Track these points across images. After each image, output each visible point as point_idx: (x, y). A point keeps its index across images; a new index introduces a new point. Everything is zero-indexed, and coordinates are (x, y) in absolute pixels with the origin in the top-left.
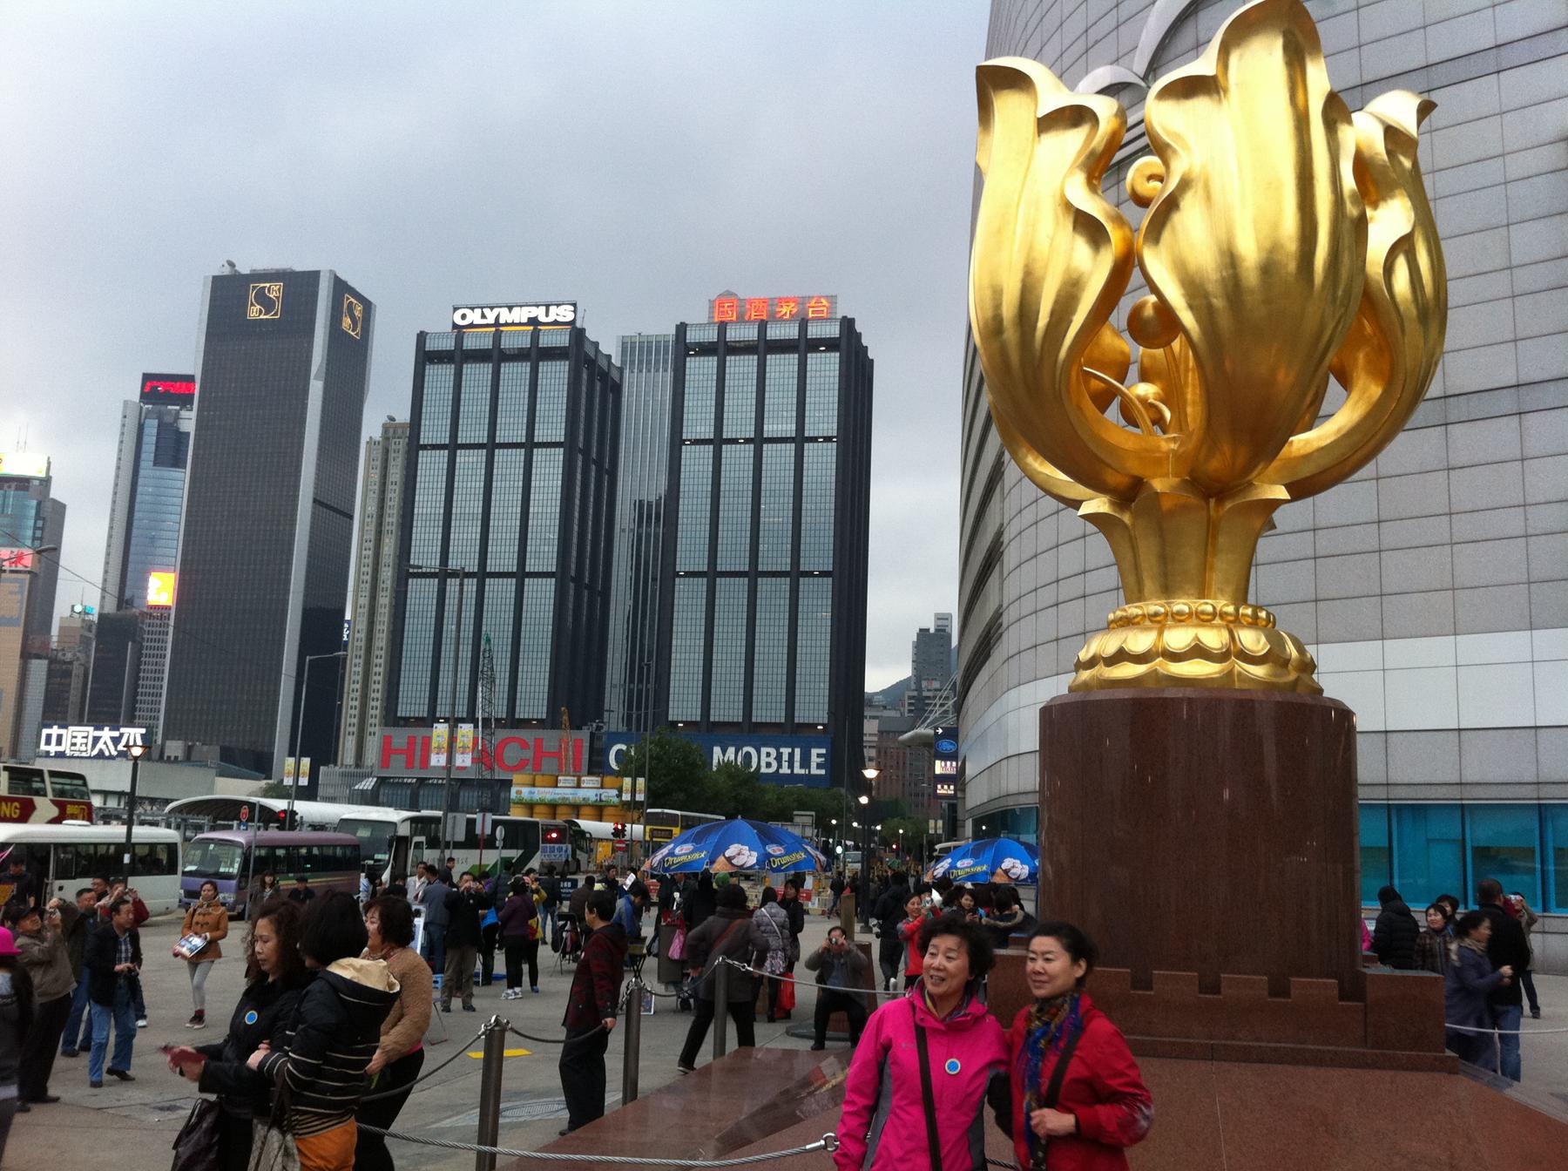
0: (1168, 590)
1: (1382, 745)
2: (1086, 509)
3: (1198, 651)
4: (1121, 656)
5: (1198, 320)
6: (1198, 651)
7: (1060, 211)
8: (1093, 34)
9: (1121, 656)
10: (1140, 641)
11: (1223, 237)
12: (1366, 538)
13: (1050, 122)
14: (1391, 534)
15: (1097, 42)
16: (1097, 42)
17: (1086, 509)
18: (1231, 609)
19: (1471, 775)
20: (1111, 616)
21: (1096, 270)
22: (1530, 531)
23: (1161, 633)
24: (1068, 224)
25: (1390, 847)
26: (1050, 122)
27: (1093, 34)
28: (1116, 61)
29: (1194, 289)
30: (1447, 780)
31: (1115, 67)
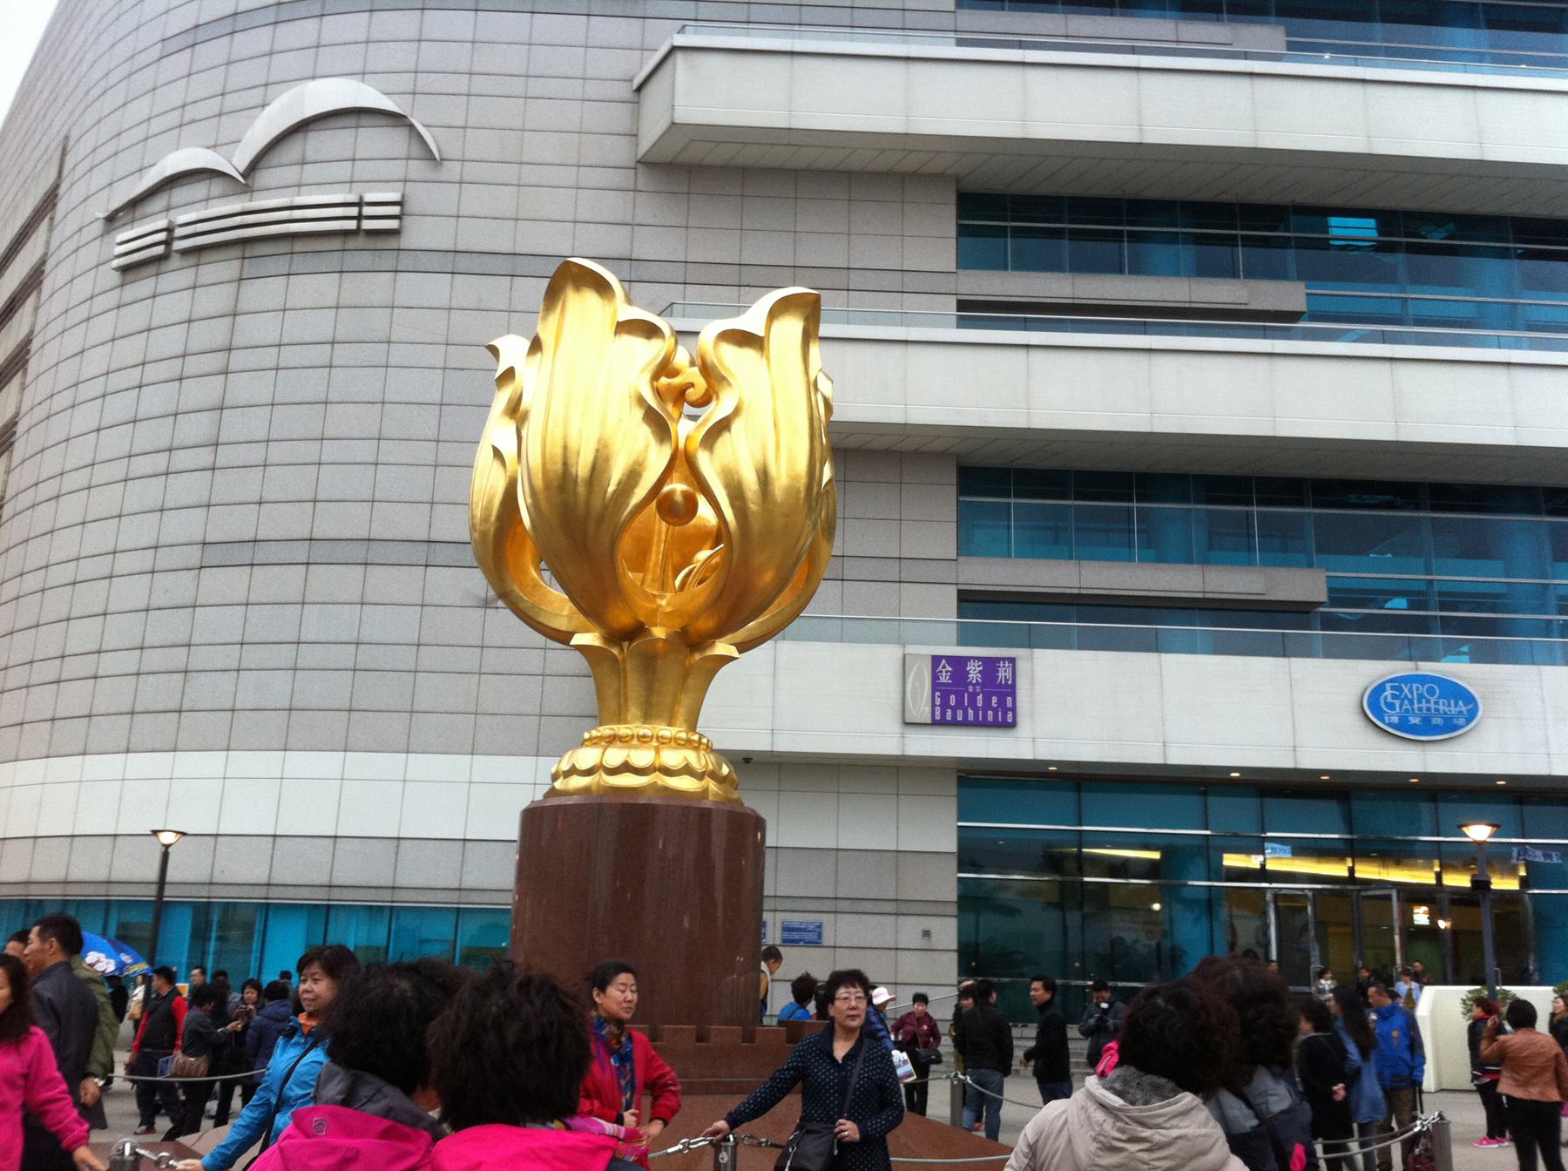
0: (647, 717)
1: (393, 850)
2: (578, 639)
3: (687, 770)
4: (626, 768)
5: (736, 515)
6: (687, 770)
7: (634, 403)
8: (191, 112)
9: (626, 768)
10: (642, 757)
11: (759, 457)
12: (406, 657)
13: (625, 327)
14: (428, 657)
15: (194, 121)
16: (194, 121)
17: (578, 639)
18: (683, 735)
19: (470, 882)
20: (587, 735)
21: (657, 459)
22: (547, 671)
23: (657, 750)
24: (639, 413)
25: (387, 947)
26: (625, 327)
27: (191, 112)
28: (214, 147)
29: (736, 492)
30: (447, 885)
31: (210, 152)
